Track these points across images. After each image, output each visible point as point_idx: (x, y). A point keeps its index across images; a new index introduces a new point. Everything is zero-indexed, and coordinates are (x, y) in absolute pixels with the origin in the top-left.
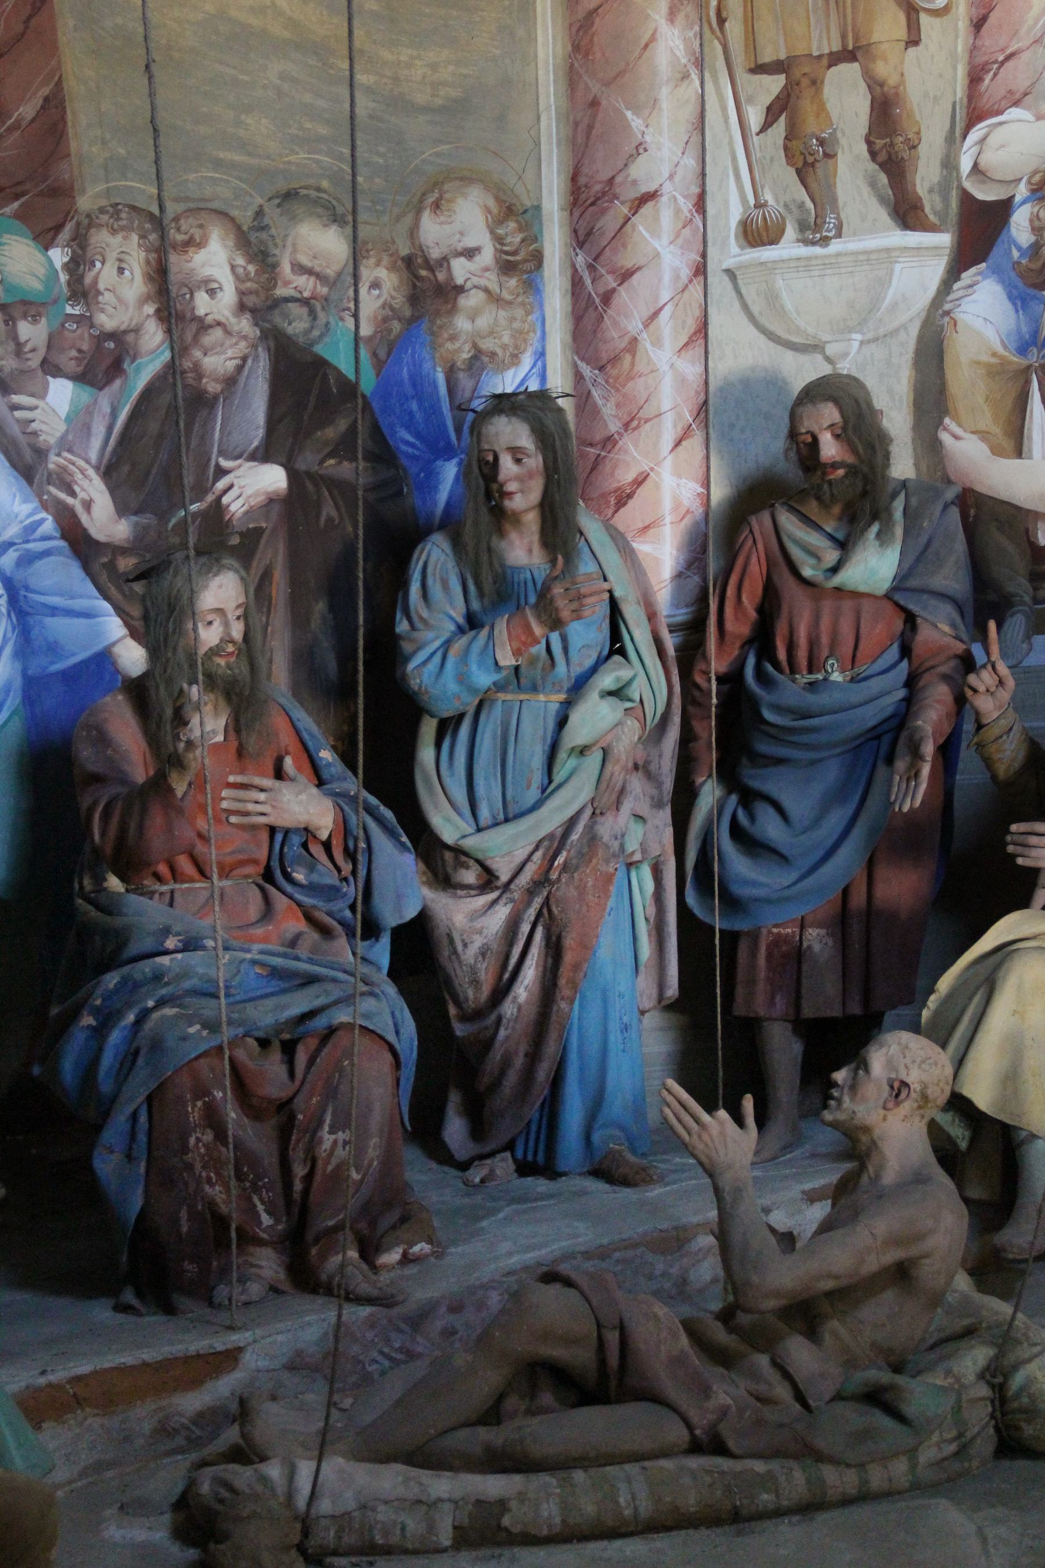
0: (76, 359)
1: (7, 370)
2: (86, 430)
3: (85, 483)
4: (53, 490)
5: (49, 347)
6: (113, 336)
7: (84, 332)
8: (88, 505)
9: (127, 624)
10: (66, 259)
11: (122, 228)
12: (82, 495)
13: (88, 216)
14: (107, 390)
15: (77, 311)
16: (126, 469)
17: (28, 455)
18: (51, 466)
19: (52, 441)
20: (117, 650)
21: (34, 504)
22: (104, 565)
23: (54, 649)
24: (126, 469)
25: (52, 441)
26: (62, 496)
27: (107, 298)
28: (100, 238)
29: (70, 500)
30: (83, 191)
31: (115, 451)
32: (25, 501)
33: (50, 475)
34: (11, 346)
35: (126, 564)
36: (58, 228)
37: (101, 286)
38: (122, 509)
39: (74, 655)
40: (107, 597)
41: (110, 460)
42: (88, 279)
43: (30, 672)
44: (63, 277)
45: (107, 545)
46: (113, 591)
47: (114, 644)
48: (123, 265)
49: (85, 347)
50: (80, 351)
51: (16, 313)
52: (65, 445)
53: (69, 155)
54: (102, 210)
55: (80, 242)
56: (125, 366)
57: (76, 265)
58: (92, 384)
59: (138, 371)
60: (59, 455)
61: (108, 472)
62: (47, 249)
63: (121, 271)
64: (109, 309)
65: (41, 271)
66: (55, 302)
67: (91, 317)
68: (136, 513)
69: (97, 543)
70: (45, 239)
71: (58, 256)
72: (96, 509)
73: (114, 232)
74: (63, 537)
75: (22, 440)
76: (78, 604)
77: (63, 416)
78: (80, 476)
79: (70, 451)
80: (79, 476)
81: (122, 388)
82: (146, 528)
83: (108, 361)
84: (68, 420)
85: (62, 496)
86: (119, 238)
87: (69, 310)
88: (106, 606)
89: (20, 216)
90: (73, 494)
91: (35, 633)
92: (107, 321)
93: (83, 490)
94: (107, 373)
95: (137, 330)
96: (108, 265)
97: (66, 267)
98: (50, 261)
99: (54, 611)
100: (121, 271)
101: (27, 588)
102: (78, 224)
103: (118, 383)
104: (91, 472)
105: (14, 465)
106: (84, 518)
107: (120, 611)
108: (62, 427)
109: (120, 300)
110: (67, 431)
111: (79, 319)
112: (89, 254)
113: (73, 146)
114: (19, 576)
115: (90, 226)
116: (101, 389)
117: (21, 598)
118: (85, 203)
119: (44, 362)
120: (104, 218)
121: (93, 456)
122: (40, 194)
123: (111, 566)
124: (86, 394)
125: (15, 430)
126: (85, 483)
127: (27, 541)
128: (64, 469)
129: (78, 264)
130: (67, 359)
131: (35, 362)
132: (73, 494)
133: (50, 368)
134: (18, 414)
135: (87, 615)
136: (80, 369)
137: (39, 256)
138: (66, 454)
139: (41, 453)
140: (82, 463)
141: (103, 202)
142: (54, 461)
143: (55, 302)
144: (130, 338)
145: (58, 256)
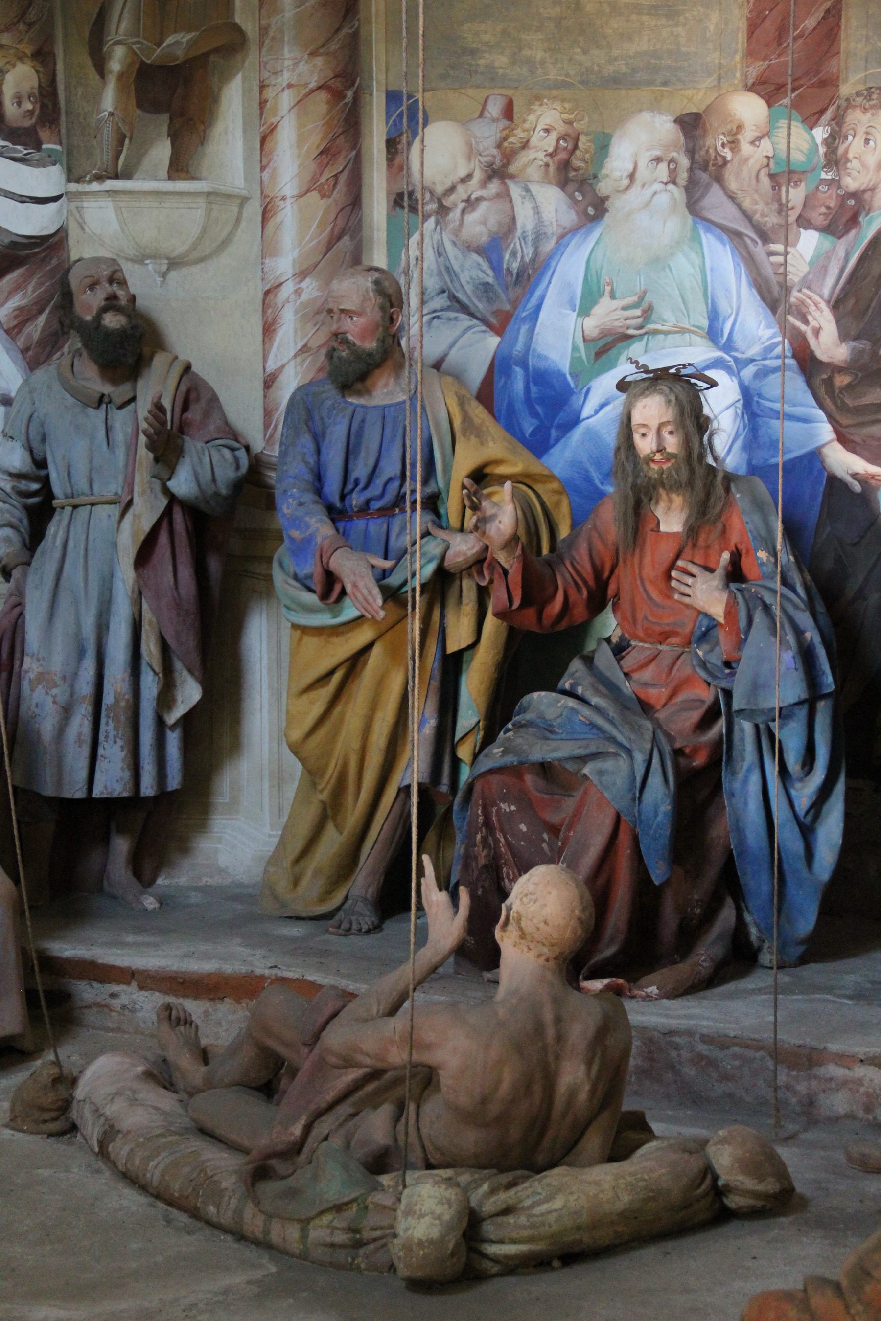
0: (824, 214)
1: (769, 225)
2: (824, 270)
3: (817, 314)
4: (791, 318)
5: (804, 206)
6: (854, 195)
7: (833, 192)
8: (817, 332)
9: (836, 431)
10: (825, 136)
11: (872, 107)
12: (813, 323)
13: (847, 100)
14: (844, 239)
15: (829, 176)
16: (851, 302)
17: (776, 289)
18: (793, 300)
19: (796, 280)
20: (826, 451)
21: (775, 329)
22: (823, 380)
23: (773, 445)
24: (851, 302)
25: (796, 280)
26: (798, 324)
27: (854, 164)
28: (857, 118)
29: (803, 327)
30: (846, 80)
31: (843, 289)
32: (769, 326)
33: (790, 306)
34: (775, 206)
35: (840, 381)
36: (822, 112)
37: (850, 155)
38: (844, 336)
39: (790, 451)
40: (821, 406)
41: (839, 295)
42: (841, 151)
43: (754, 462)
44: (822, 150)
45: (828, 364)
46: (828, 402)
47: (824, 446)
48: (869, 137)
49: (832, 205)
50: (828, 208)
51: (783, 180)
52: (806, 283)
53: (838, 53)
54: (858, 94)
55: (838, 120)
56: (861, 219)
57: (832, 142)
58: (833, 234)
59: (870, 223)
60: (800, 291)
61: (836, 305)
62: (811, 129)
63: (867, 141)
64: (855, 174)
65: (805, 146)
66: (814, 169)
67: (839, 180)
68: (855, 339)
69: (821, 363)
70: (811, 122)
71: (820, 133)
72: (823, 335)
73: (865, 110)
74: (794, 356)
75: (774, 279)
76: (798, 411)
77: (808, 260)
78: (814, 308)
79: (809, 288)
80: (812, 308)
81: (856, 236)
82: (861, 352)
83: (849, 215)
84: (811, 264)
85: (798, 324)
86: (869, 115)
87: (824, 176)
88: (821, 414)
89: (795, 105)
90: (806, 322)
91: (762, 432)
92: (851, 183)
93: (815, 319)
94: (846, 225)
95: (873, 190)
96: (857, 138)
97: (826, 142)
98: (813, 138)
99: (776, 415)
100: (867, 141)
101: (760, 395)
102: (839, 107)
103: (853, 233)
104: (823, 305)
105: (763, 299)
106: (812, 342)
107: (831, 419)
108: (806, 269)
109: (864, 166)
110: (809, 272)
111: (830, 183)
112: (844, 130)
113: (843, 45)
114: (755, 386)
115: (847, 108)
116: (839, 238)
117: (754, 403)
118: (846, 90)
119: (800, 217)
120: (859, 100)
121: (826, 292)
122: (813, 86)
123: (829, 383)
124: (828, 242)
125: (769, 271)
126: (817, 314)
127: (765, 359)
128: (802, 302)
129: (835, 139)
130: (818, 216)
131: (793, 217)
132: (806, 322)
133: (804, 222)
134: (773, 259)
135: (805, 420)
136: (826, 223)
137: (806, 136)
138: (805, 291)
139: (787, 290)
140: (816, 298)
141: (861, 87)
142: (795, 296)
143: (814, 169)
144: (867, 196)
145: (820, 133)
